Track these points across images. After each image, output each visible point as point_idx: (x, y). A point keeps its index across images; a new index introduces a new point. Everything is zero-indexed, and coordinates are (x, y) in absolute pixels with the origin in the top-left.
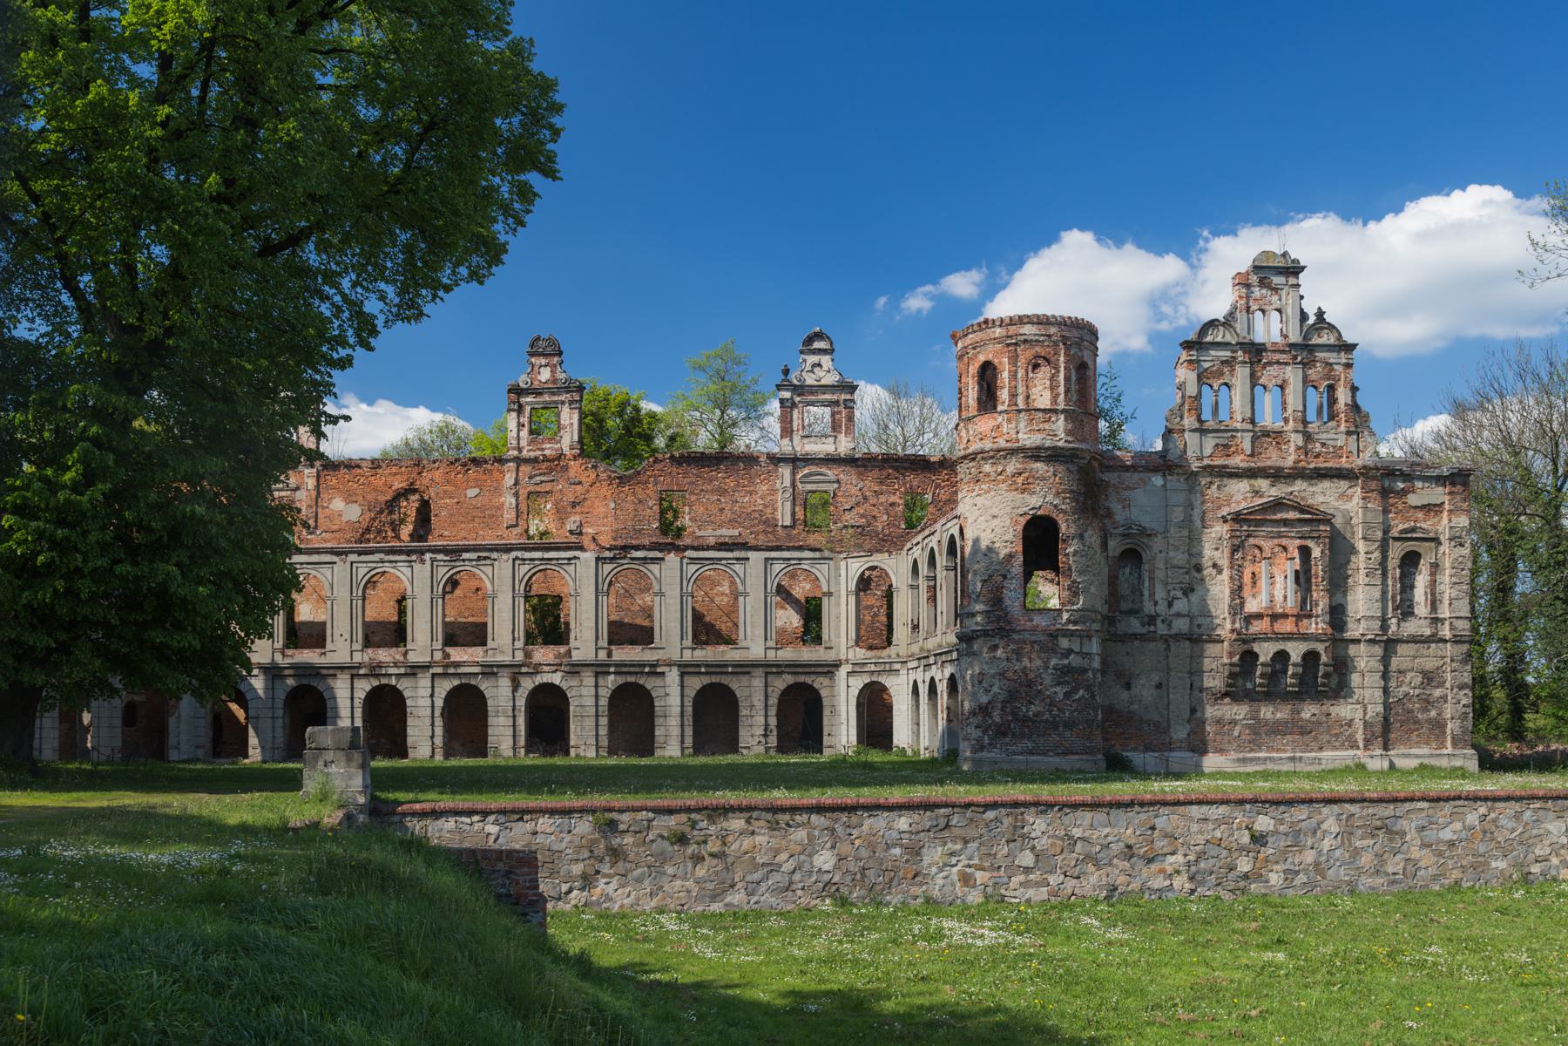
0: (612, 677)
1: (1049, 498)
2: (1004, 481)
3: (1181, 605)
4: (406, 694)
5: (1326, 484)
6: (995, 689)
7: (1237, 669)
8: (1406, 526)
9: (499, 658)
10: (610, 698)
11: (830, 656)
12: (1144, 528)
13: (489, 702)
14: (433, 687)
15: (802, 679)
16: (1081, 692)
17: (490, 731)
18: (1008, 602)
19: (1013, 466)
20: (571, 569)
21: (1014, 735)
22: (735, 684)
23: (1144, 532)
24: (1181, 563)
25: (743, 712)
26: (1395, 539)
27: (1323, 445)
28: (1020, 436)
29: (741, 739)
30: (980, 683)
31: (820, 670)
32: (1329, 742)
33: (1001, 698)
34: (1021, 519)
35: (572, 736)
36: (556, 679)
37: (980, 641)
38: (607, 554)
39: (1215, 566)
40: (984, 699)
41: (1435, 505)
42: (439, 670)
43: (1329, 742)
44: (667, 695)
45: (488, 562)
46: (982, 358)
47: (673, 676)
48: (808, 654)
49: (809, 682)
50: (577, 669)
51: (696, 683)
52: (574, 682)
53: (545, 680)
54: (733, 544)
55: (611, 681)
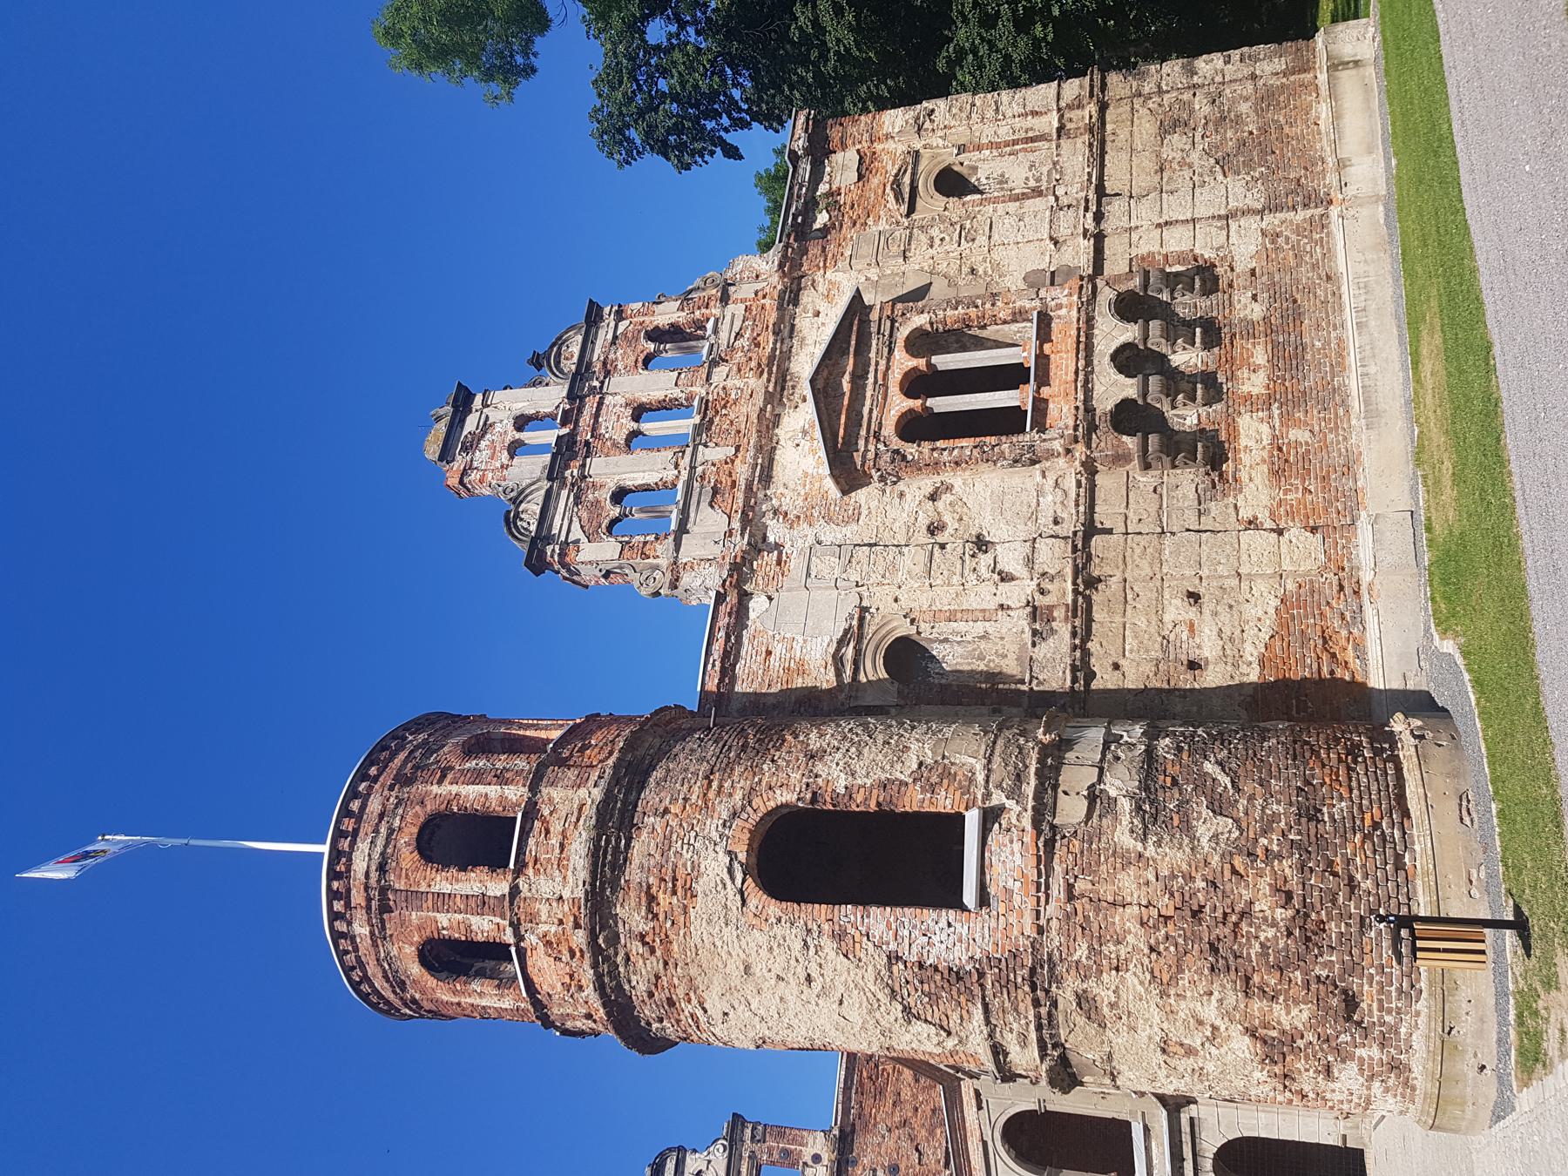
1: (712, 827)
2: (667, 941)
3: (1011, 560)
5: (804, 322)
6: (1210, 1012)
7: (1153, 440)
8: (891, 197)
12: (846, 632)
16: (1209, 767)
18: (959, 957)
19: (630, 915)
21: (1353, 968)
23: (854, 634)
24: (922, 557)
26: (911, 209)
27: (738, 335)
28: (566, 894)
30: (1190, 1052)
32: (1315, 266)
33: (1231, 999)
34: (752, 903)
39: (933, 497)
40: (1241, 1046)
41: (860, 163)
43: (1315, 266)
46: (415, 969)
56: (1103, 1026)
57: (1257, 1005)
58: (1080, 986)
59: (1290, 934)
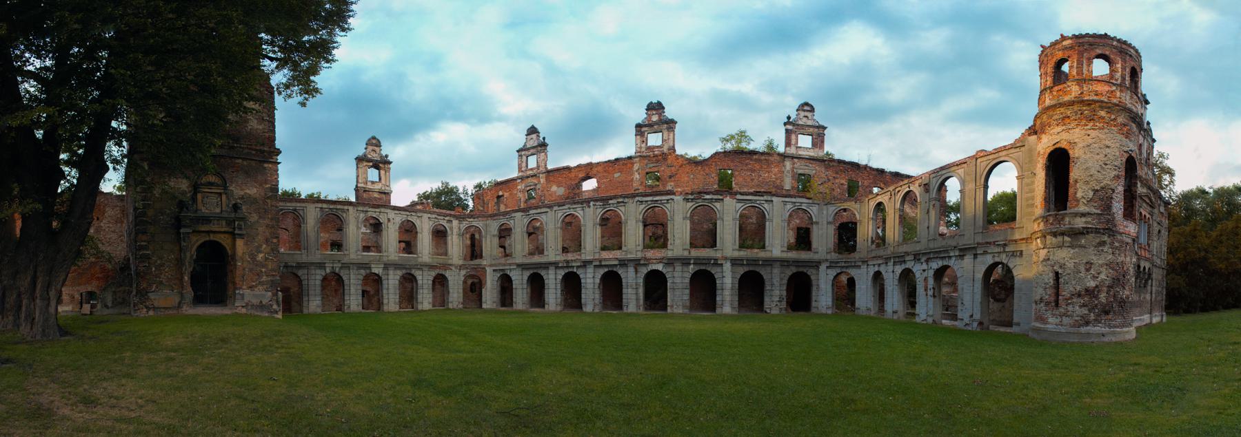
0: (692, 266)
4: (581, 276)
6: (1103, 276)
9: (630, 256)
10: (691, 278)
11: (816, 257)
13: (624, 281)
14: (594, 273)
15: (801, 269)
17: (624, 296)
20: (667, 205)
22: (764, 272)
25: (768, 287)
29: (765, 303)
31: (811, 264)
35: (669, 300)
36: (660, 267)
37: (1090, 236)
38: (690, 197)
42: (598, 263)
44: (723, 277)
45: (623, 204)
47: (727, 266)
48: (803, 255)
49: (805, 271)
50: (671, 262)
51: (741, 271)
52: (670, 269)
53: (654, 268)
54: (764, 192)
55: (692, 268)
56: (1095, 247)
57: (1105, 289)
58: (1108, 242)
59: (1121, 298)
